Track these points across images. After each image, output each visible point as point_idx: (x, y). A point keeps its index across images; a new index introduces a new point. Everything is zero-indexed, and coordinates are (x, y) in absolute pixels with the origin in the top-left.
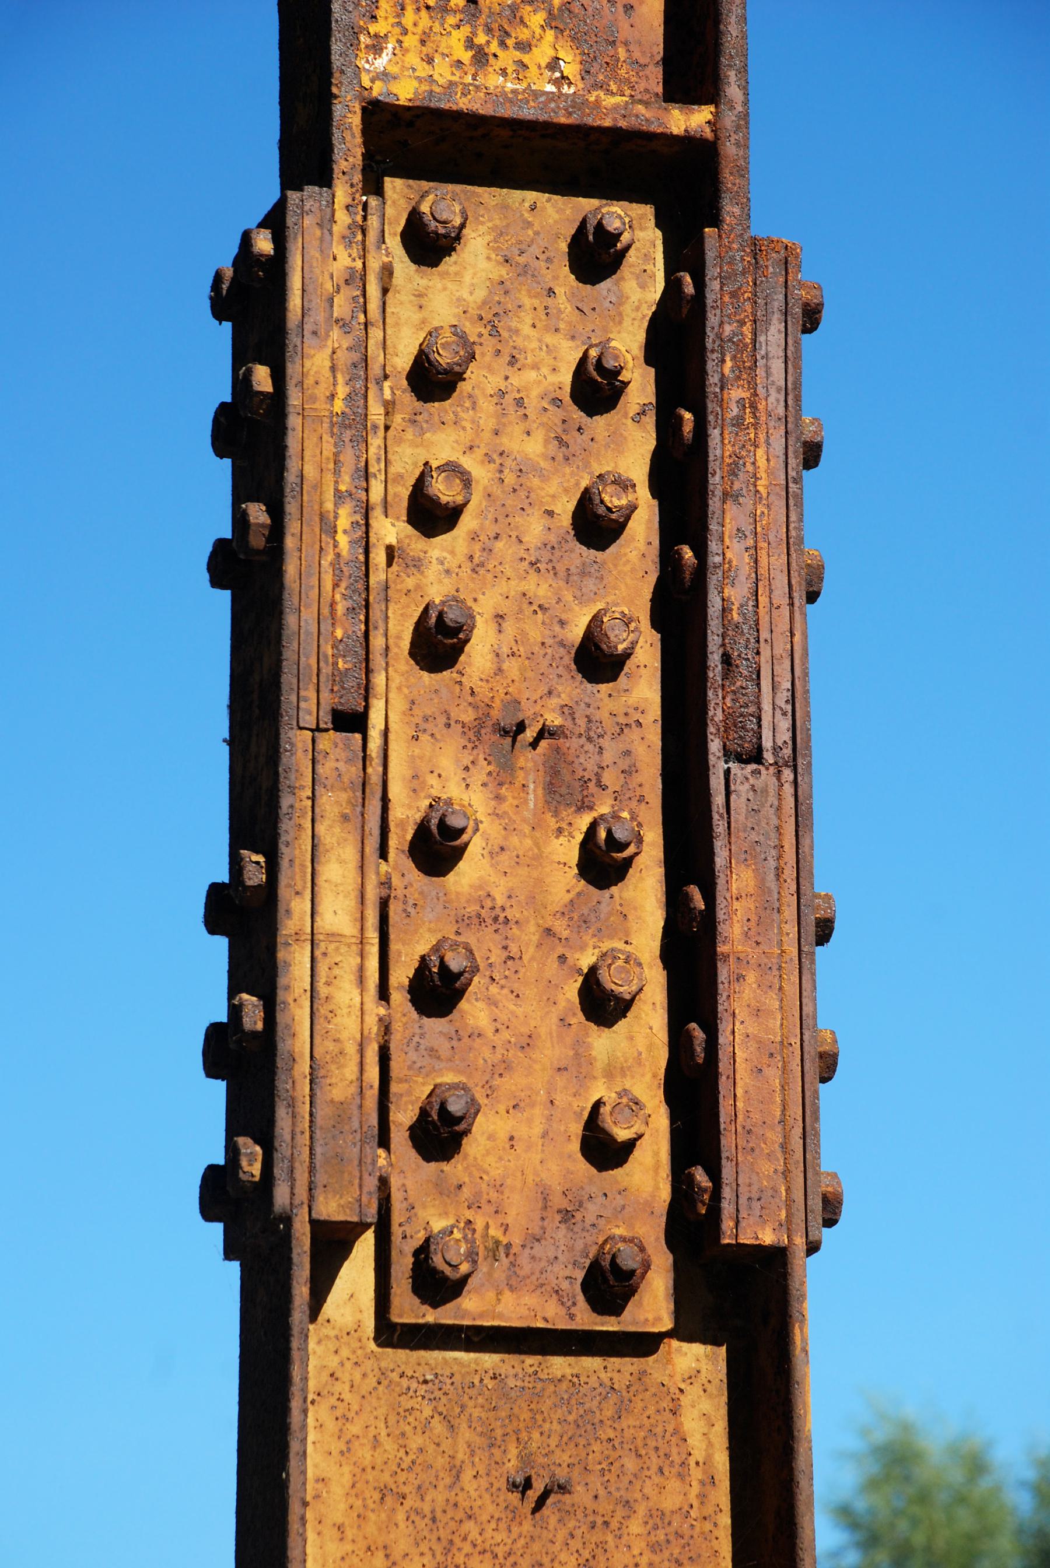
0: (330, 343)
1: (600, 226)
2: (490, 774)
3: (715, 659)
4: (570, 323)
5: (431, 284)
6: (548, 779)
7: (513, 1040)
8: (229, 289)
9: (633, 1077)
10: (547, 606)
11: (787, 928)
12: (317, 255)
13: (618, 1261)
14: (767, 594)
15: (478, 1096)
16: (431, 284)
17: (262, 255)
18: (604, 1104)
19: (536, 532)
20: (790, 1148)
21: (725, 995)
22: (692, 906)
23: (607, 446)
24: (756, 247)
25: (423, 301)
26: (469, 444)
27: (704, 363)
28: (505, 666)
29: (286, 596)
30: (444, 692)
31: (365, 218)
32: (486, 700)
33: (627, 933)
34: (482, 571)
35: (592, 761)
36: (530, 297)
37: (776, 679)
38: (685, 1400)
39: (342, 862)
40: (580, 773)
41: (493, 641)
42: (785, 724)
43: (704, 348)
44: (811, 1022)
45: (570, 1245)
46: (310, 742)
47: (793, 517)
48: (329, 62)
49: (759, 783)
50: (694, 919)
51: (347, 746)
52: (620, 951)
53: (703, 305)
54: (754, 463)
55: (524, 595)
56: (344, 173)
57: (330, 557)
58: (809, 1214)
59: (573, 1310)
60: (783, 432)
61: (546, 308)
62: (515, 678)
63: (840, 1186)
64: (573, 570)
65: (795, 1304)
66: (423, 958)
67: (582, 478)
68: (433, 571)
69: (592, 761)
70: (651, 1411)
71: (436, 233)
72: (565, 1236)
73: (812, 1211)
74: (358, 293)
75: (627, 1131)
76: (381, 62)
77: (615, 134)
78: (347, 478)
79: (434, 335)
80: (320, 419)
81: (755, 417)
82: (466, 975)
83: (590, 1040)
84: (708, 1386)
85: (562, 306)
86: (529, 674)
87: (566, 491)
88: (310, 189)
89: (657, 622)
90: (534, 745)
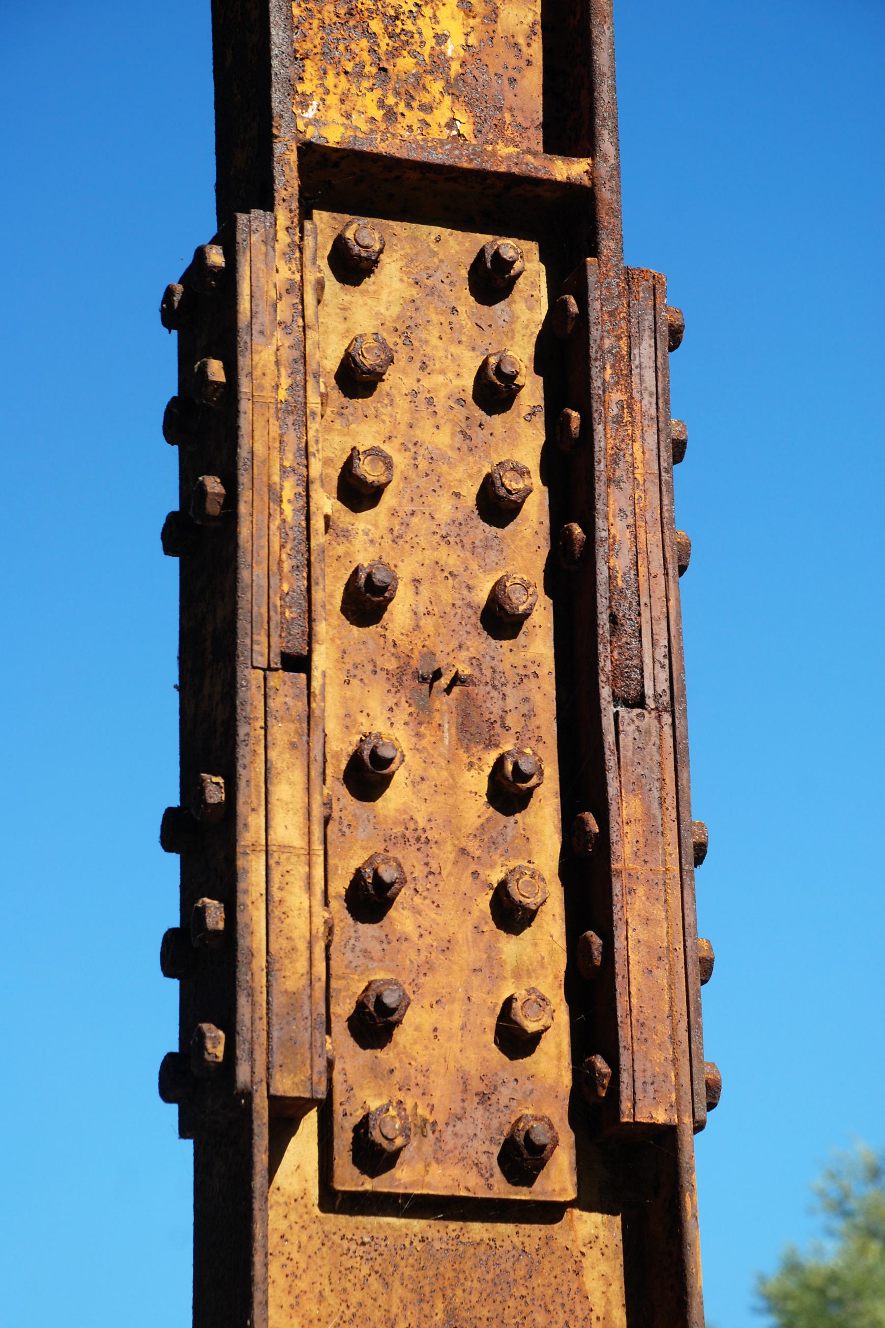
0: (274, 341)
1: (497, 255)
2: (411, 714)
3: (603, 618)
4: (471, 336)
5: (353, 300)
6: (460, 720)
7: (435, 944)
8: (180, 302)
9: (537, 978)
10: (456, 573)
11: (669, 849)
12: (263, 267)
13: (532, 1136)
14: (646, 564)
15: (407, 992)
16: (353, 300)
17: (215, 267)
18: (516, 999)
19: (446, 510)
20: (677, 1039)
21: (619, 906)
22: (588, 829)
23: (504, 440)
24: (629, 276)
25: (347, 314)
26: (388, 435)
27: (588, 369)
28: (422, 623)
29: (240, 553)
30: (371, 645)
31: (302, 239)
32: (406, 651)
33: (530, 855)
34: (401, 542)
35: (497, 706)
36: (437, 314)
37: (655, 636)
38: (586, 1262)
39: (291, 784)
40: (487, 716)
41: (412, 602)
42: (663, 675)
43: (588, 357)
44: (692, 930)
45: (487, 1123)
46: (262, 680)
47: (666, 501)
48: (270, 108)
49: (643, 725)
50: (590, 842)
51: (294, 684)
52: (526, 868)
53: (587, 321)
54: (632, 455)
55: (437, 563)
56: (284, 200)
57: (278, 522)
58: (695, 1097)
59: (491, 1181)
60: (655, 430)
61: (450, 323)
62: (430, 633)
63: (719, 1074)
64: (478, 543)
65: (685, 1176)
66: (358, 871)
67: (484, 466)
68: (359, 541)
69: (497, 706)
70: (558, 1271)
71: (359, 256)
72: (483, 1116)
73: (698, 1095)
74: (297, 301)
75: (536, 1024)
76: (310, 114)
77: (508, 178)
78: (290, 456)
79: (359, 340)
80: (267, 405)
81: (632, 416)
82: (396, 885)
83: (500, 945)
84: (605, 1250)
85: (463, 322)
86: (443, 630)
87: (470, 476)
88: (256, 213)
89: (549, 590)
90: (448, 690)
